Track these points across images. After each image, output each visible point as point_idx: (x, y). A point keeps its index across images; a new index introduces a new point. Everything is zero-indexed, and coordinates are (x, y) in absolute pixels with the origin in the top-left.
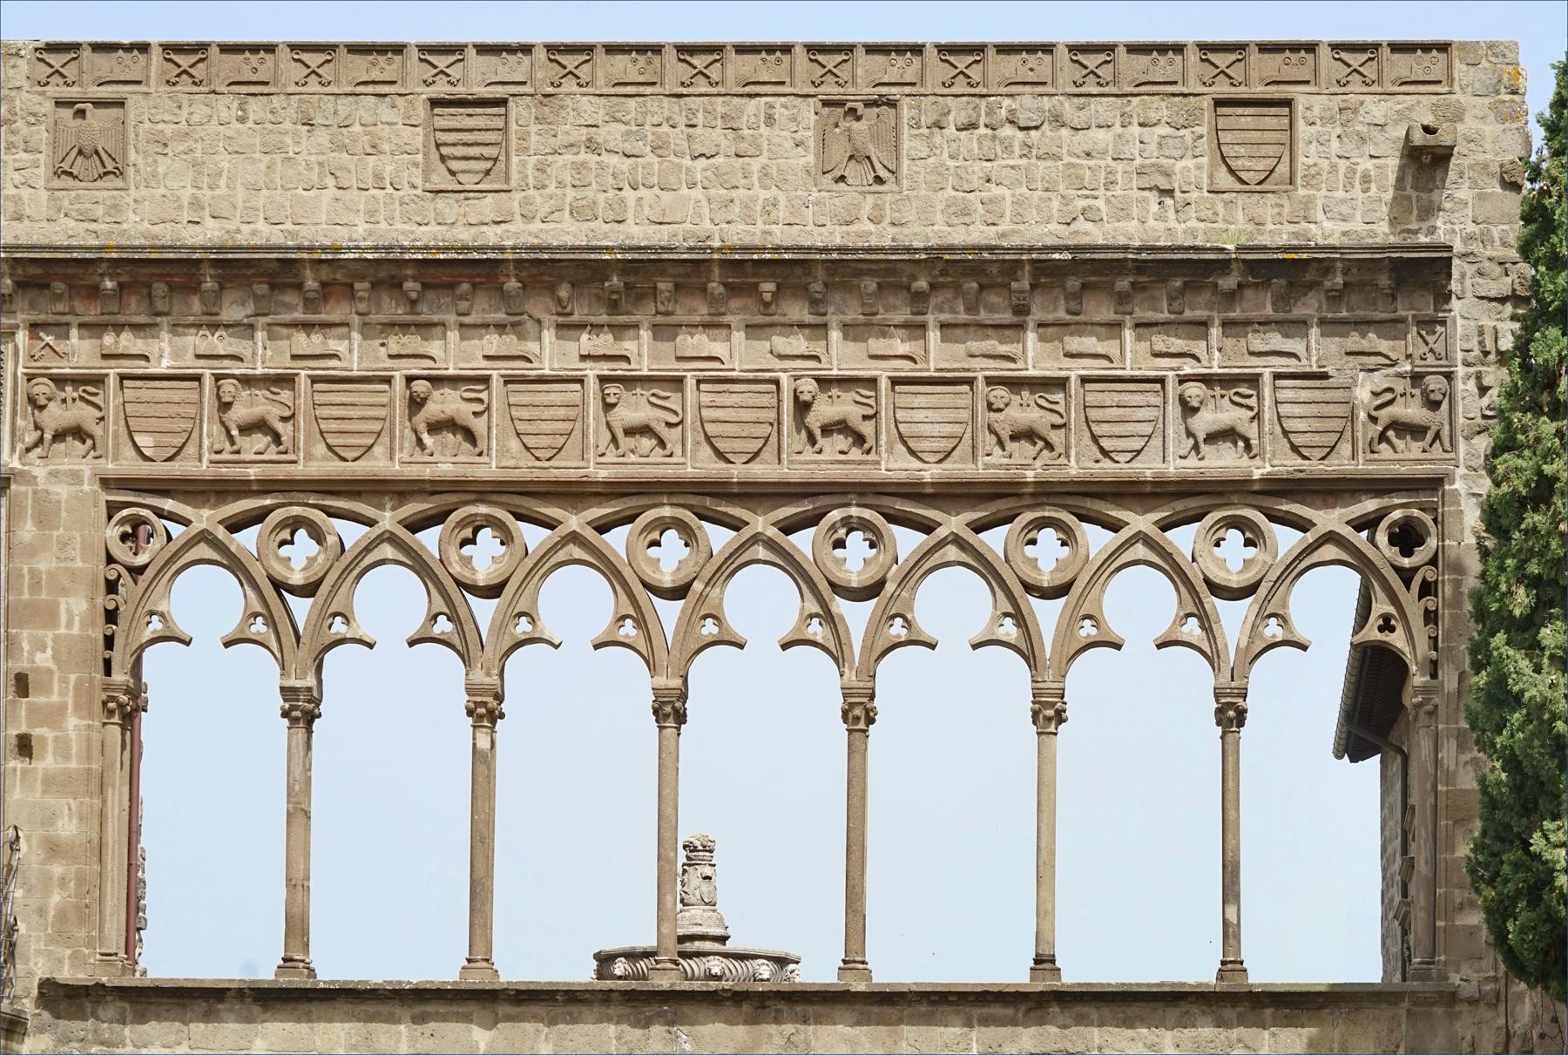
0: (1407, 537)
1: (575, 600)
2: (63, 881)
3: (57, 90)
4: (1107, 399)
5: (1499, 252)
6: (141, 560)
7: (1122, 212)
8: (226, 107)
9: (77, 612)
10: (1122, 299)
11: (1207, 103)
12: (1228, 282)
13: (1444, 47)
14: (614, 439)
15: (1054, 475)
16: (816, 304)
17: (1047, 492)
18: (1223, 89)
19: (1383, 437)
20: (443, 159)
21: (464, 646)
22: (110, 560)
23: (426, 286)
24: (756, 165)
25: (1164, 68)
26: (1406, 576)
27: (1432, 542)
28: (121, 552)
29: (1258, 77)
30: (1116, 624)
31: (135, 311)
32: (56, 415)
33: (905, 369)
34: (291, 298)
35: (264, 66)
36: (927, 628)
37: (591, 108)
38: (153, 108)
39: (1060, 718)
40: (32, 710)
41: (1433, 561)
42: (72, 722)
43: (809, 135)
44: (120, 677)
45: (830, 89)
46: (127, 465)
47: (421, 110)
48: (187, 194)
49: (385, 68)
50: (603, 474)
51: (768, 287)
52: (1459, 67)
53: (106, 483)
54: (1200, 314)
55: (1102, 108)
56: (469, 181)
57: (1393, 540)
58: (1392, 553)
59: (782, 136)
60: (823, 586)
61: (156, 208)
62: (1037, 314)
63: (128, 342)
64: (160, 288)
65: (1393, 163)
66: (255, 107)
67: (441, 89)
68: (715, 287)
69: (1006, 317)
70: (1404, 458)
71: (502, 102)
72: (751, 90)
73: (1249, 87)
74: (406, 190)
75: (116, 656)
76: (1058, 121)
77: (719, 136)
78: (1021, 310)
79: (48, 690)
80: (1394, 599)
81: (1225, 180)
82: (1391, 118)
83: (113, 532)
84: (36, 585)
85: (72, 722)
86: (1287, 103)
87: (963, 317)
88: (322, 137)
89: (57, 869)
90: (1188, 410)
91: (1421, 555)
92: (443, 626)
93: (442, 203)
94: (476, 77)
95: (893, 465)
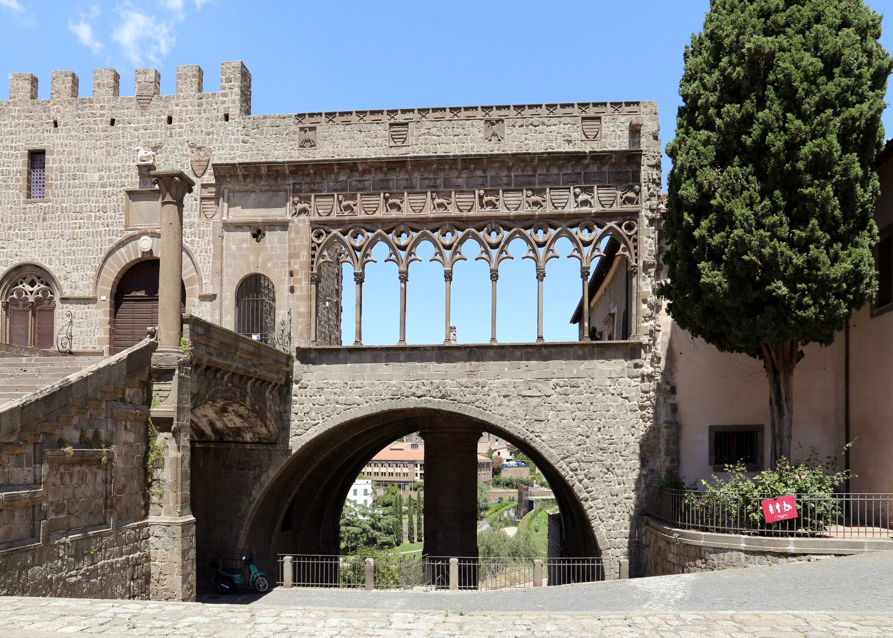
0: (629, 227)
1: (425, 249)
2: (302, 323)
3: (300, 125)
4: (556, 193)
5: (653, 154)
6: (320, 242)
7: (559, 146)
8: (341, 128)
9: (305, 255)
10: (560, 168)
11: (580, 118)
12: (587, 161)
13: (638, 103)
14: (434, 208)
15: (543, 213)
16: (484, 171)
17: (542, 217)
18: (584, 114)
19: (624, 203)
20: (393, 139)
21: (398, 261)
22: (313, 242)
23: (389, 169)
24: (469, 137)
25: (568, 110)
26: (630, 237)
27: (636, 229)
28: (315, 240)
29: (591, 112)
30: (557, 252)
31: (318, 179)
33: (506, 188)
34: (356, 174)
35: (350, 118)
36: (511, 254)
37: (429, 124)
38: (323, 127)
39: (544, 275)
40: (294, 280)
41: (636, 233)
42: (304, 282)
43: (482, 130)
44: (315, 271)
45: (487, 117)
46: (317, 218)
47: (388, 126)
48: (331, 150)
49: (379, 117)
50: (432, 216)
51: (472, 166)
52: (642, 108)
53: (311, 222)
54: (579, 171)
55: (554, 121)
56: (399, 144)
57: (626, 228)
58: (626, 231)
59: (475, 130)
60: (486, 243)
61: (323, 152)
62: (539, 171)
63: (316, 187)
64: (324, 172)
65: (626, 133)
66: (348, 128)
67: (392, 121)
68: (459, 167)
69: (531, 173)
70: (629, 208)
71: (407, 124)
72: (468, 118)
73: (590, 113)
74: (384, 147)
75: (314, 266)
76: (543, 124)
77: (460, 130)
78: (535, 171)
79: (297, 275)
80: (626, 243)
81: (584, 138)
82: (624, 120)
84: (295, 249)
85: (304, 282)
86: (599, 118)
87: (520, 173)
88: (363, 134)
89: (300, 320)
90: (576, 196)
91: (633, 232)
92: (393, 257)
93: (392, 149)
94: (400, 118)
95: (502, 211)
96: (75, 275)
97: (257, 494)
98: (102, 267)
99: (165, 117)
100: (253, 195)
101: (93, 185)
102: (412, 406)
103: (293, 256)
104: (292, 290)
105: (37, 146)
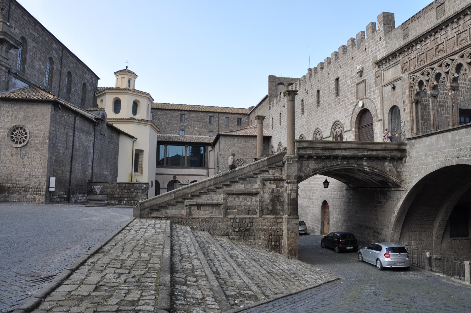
32: (404, 69)
83: (412, 80)
96: (347, 122)
97: (396, 213)
98: (352, 117)
99: (364, 49)
100: (391, 70)
101: (349, 86)
102: (454, 164)
103: (404, 93)
104: (405, 110)
105: (336, 77)
